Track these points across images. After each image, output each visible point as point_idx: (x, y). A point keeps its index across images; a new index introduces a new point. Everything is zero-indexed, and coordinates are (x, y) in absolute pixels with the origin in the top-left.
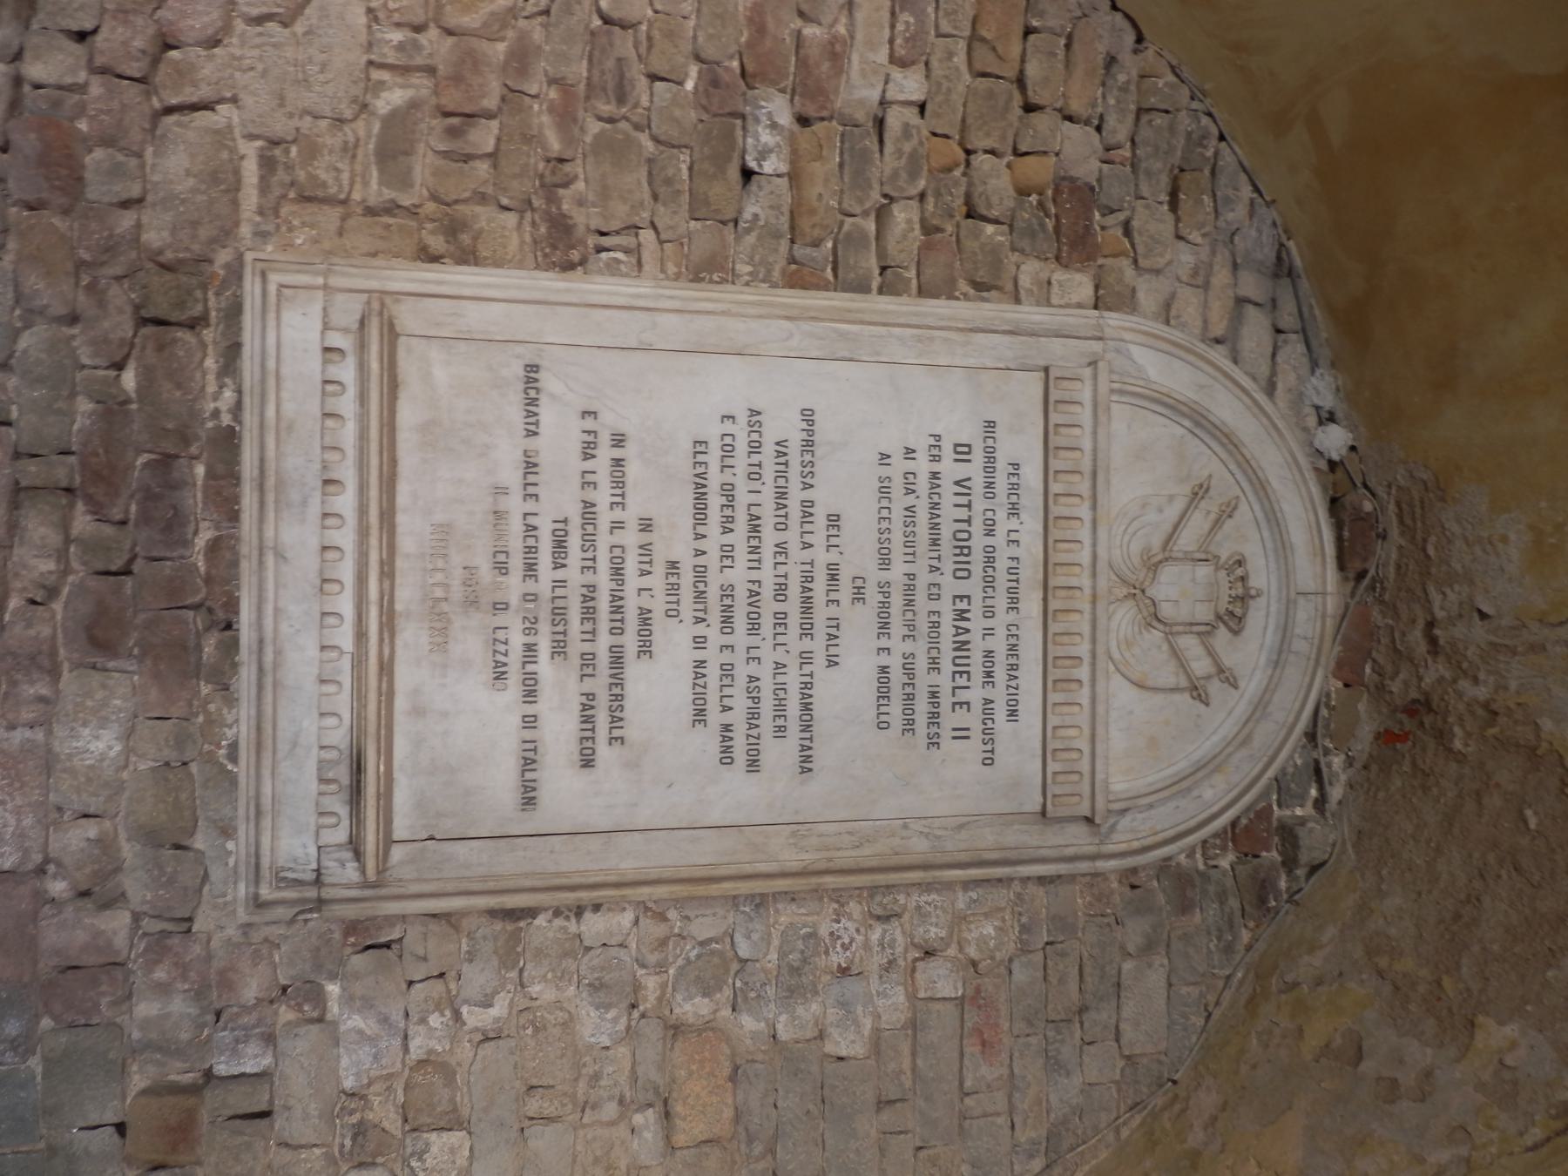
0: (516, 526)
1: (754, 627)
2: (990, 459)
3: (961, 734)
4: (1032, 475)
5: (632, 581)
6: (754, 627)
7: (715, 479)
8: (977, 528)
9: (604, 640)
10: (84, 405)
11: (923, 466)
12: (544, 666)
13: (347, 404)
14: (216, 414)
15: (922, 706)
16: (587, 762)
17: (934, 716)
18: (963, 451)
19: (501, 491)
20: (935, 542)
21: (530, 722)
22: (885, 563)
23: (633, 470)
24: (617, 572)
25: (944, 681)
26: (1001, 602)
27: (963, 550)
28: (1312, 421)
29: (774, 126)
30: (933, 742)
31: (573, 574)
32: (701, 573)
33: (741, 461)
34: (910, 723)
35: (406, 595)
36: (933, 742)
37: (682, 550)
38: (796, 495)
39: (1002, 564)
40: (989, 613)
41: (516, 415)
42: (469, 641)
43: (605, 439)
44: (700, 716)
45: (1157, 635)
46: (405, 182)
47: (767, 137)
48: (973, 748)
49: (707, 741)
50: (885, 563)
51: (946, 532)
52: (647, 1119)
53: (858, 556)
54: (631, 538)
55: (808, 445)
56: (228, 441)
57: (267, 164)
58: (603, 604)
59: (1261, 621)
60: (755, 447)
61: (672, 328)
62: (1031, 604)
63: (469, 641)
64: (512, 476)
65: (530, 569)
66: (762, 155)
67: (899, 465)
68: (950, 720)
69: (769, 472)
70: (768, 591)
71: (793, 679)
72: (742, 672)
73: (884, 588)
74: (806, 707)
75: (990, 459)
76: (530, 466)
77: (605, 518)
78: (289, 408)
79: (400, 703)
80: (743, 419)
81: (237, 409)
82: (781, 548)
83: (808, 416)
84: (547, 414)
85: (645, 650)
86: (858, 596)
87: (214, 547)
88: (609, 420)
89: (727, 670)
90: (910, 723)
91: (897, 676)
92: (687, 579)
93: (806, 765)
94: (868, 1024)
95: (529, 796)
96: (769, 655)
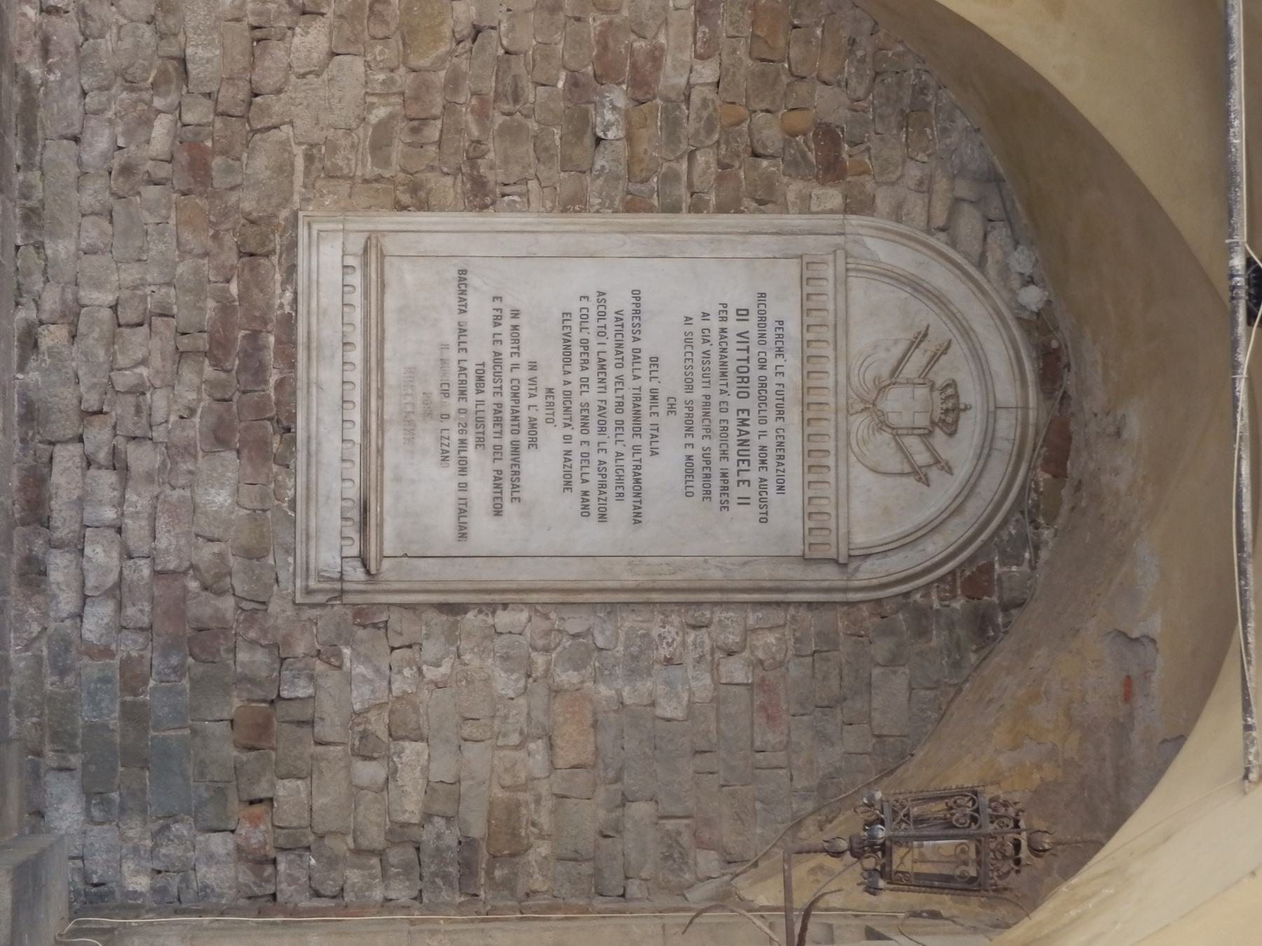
0: (454, 368)
1: (602, 429)
2: (762, 319)
3: (744, 502)
4: (793, 329)
5: (525, 401)
6: (602, 429)
7: (576, 336)
8: (754, 364)
9: (507, 438)
10: (211, 303)
11: (715, 324)
12: (471, 453)
13: (356, 298)
14: (281, 306)
15: (716, 483)
16: (498, 512)
17: (725, 489)
18: (743, 314)
19: (444, 347)
20: (724, 374)
21: (463, 487)
22: (689, 388)
23: (524, 333)
24: (515, 395)
25: (732, 466)
26: (771, 414)
27: (744, 379)
28: (1015, 283)
29: (614, 108)
30: (724, 506)
31: (488, 396)
32: (568, 395)
33: (593, 324)
34: (707, 494)
35: (390, 409)
36: (724, 506)
37: (555, 381)
38: (629, 345)
39: (772, 388)
40: (763, 421)
41: (453, 301)
42: (427, 437)
43: (507, 313)
44: (568, 485)
45: (886, 436)
46: (387, 163)
47: (609, 116)
48: (753, 511)
49: (572, 502)
50: (689, 388)
51: (732, 367)
52: (537, 746)
53: (671, 382)
54: (523, 374)
55: (637, 313)
56: (289, 323)
57: (309, 158)
58: (507, 415)
59: (970, 427)
60: (602, 316)
61: (548, 243)
62: (793, 415)
63: (427, 437)
64: (451, 339)
65: (463, 393)
66: (607, 128)
67: (698, 324)
68: (736, 492)
69: (611, 331)
70: (611, 406)
71: (628, 463)
72: (595, 458)
73: (689, 405)
74: (637, 481)
75: (762, 319)
76: (462, 331)
77: (507, 361)
78: (324, 301)
79: (388, 474)
80: (594, 298)
81: (295, 300)
82: (620, 380)
83: (636, 294)
84: (472, 299)
85: (533, 443)
86: (672, 410)
87: (280, 384)
88: (509, 302)
89: (585, 456)
90: (707, 494)
91: (698, 462)
92: (559, 400)
93: (637, 519)
94: (685, 697)
95: (463, 535)
96: (612, 448)
